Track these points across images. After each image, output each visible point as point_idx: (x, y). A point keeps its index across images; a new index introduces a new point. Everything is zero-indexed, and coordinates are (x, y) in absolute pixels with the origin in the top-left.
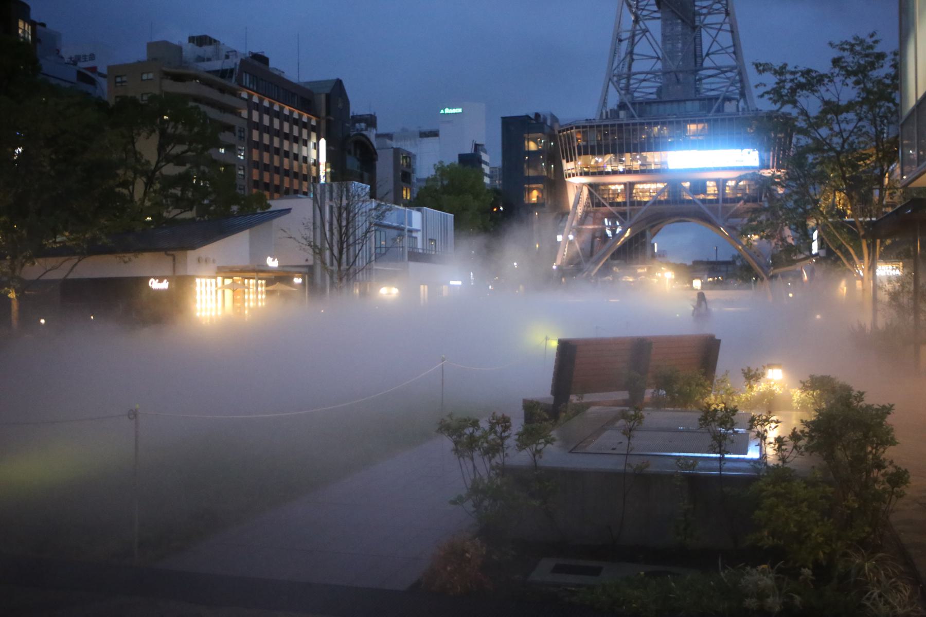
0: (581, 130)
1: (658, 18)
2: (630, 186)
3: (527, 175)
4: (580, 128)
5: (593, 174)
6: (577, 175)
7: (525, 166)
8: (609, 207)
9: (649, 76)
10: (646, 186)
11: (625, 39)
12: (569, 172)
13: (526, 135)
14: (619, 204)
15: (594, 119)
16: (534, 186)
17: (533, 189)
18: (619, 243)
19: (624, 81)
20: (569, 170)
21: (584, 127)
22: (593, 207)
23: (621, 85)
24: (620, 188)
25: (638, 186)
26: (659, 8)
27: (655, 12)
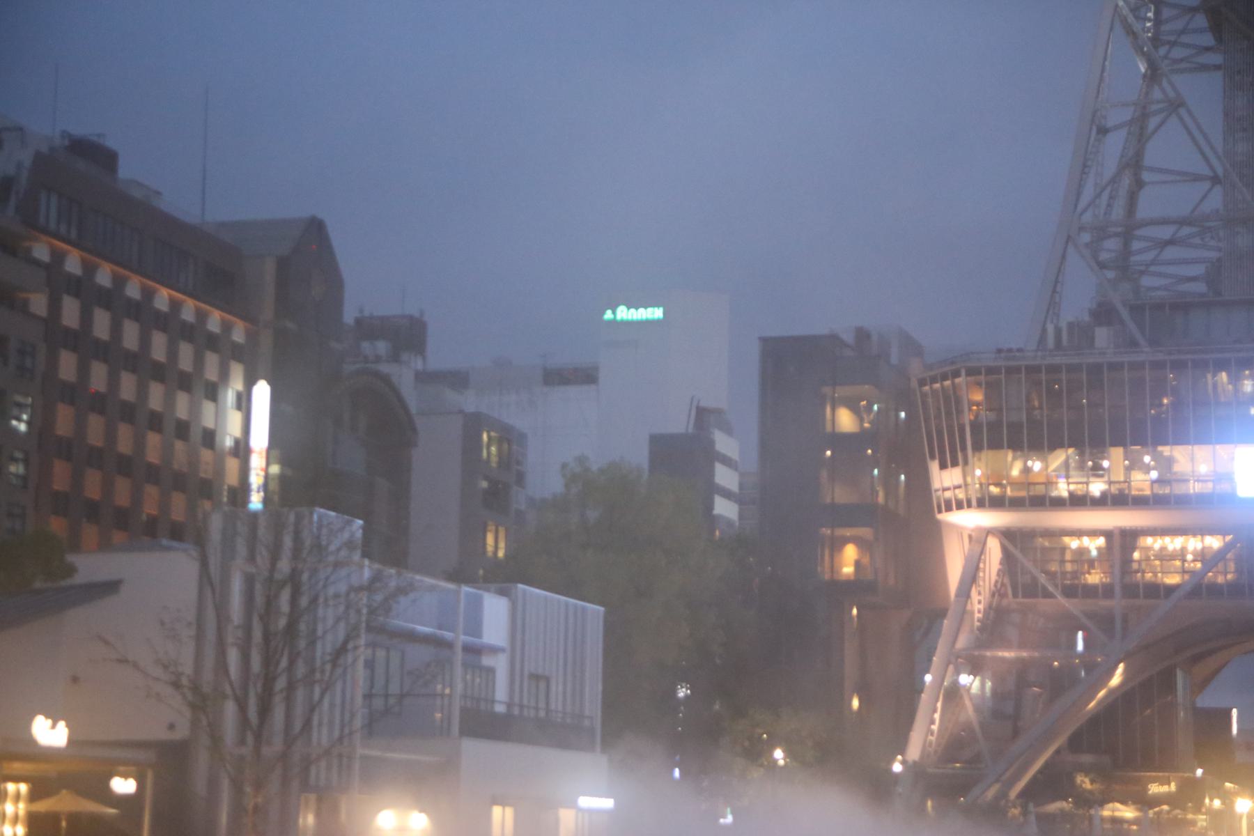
0: (982, 378)
1: (1217, 67)
2: (1124, 540)
3: (828, 500)
4: (979, 373)
5: (1016, 504)
6: (969, 506)
7: (824, 474)
8: (1061, 599)
9: (1186, 231)
10: (1173, 543)
11: (1116, 128)
12: (948, 494)
13: (827, 390)
14: (1091, 591)
15: (1019, 350)
16: (848, 532)
17: (846, 541)
18: (1092, 704)
19: (1112, 244)
20: (948, 489)
21: (990, 371)
22: (1015, 595)
23: (1104, 256)
24: (1094, 545)
25: (1154, 543)
26: (1219, 39)
27: (1208, 49)
